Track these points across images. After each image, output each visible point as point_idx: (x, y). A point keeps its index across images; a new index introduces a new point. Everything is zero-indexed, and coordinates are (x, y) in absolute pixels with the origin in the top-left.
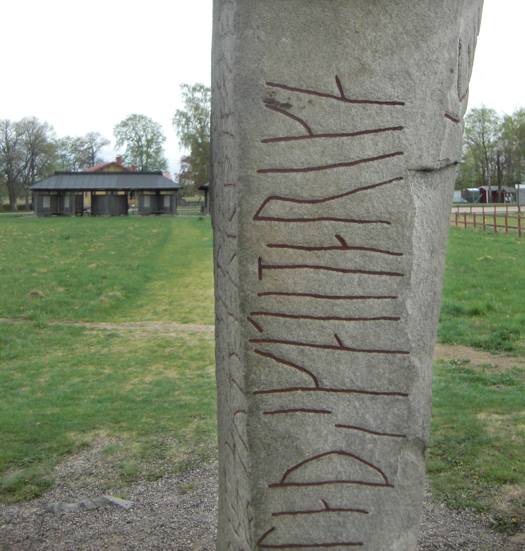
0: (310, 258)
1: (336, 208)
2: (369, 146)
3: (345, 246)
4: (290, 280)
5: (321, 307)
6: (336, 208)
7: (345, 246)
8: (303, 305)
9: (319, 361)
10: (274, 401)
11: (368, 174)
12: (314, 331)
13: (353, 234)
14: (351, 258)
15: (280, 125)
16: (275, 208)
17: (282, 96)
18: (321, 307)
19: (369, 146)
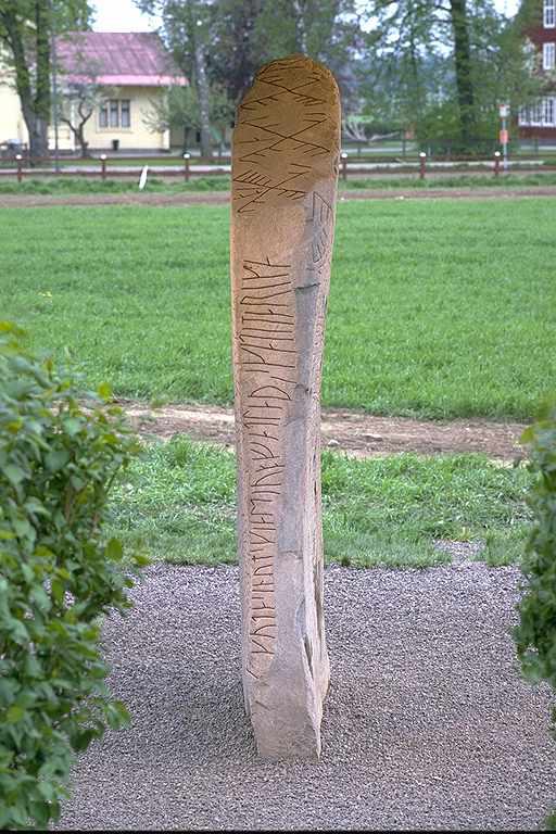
0: (259, 317)
1: (268, 301)
2: (280, 280)
3: (272, 314)
4: (254, 324)
5: (265, 334)
6: (268, 301)
7: (272, 314)
8: (255, 333)
9: (265, 354)
10: (247, 366)
11: (276, 290)
12: (258, 342)
13: (275, 310)
14: (275, 318)
15: (248, 274)
16: (246, 300)
17: (249, 265)
18: (265, 334)
19: (280, 280)
